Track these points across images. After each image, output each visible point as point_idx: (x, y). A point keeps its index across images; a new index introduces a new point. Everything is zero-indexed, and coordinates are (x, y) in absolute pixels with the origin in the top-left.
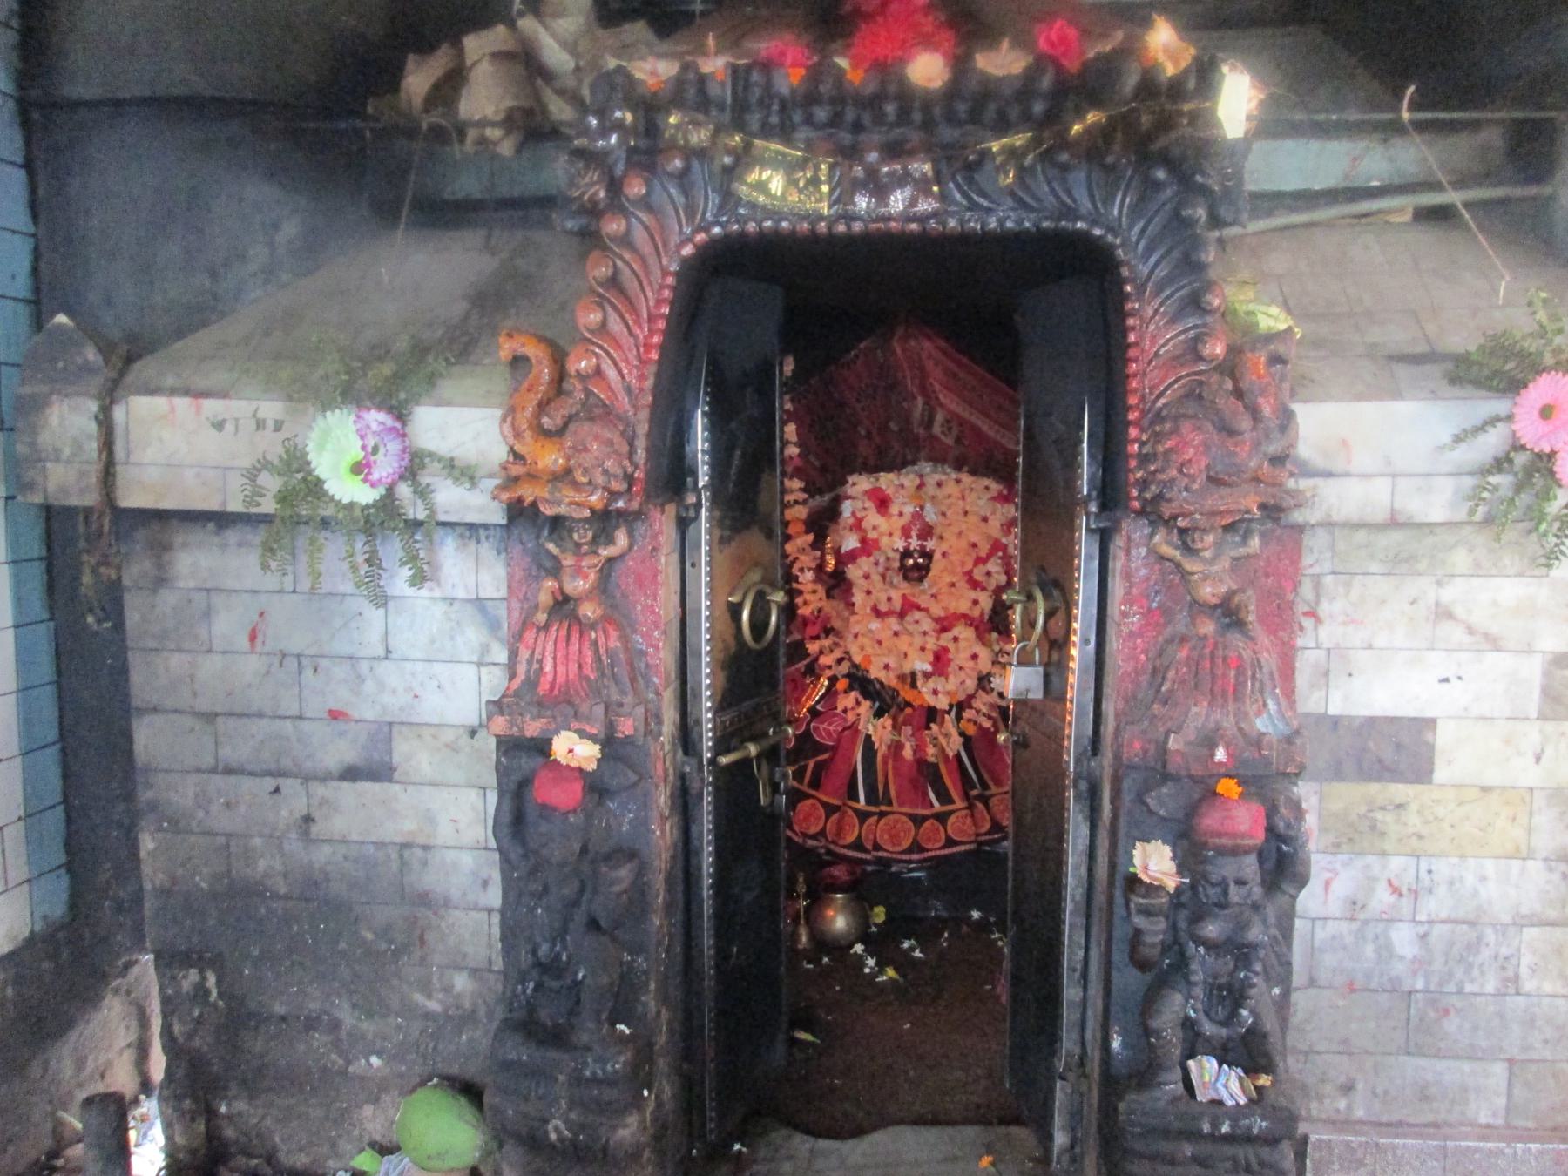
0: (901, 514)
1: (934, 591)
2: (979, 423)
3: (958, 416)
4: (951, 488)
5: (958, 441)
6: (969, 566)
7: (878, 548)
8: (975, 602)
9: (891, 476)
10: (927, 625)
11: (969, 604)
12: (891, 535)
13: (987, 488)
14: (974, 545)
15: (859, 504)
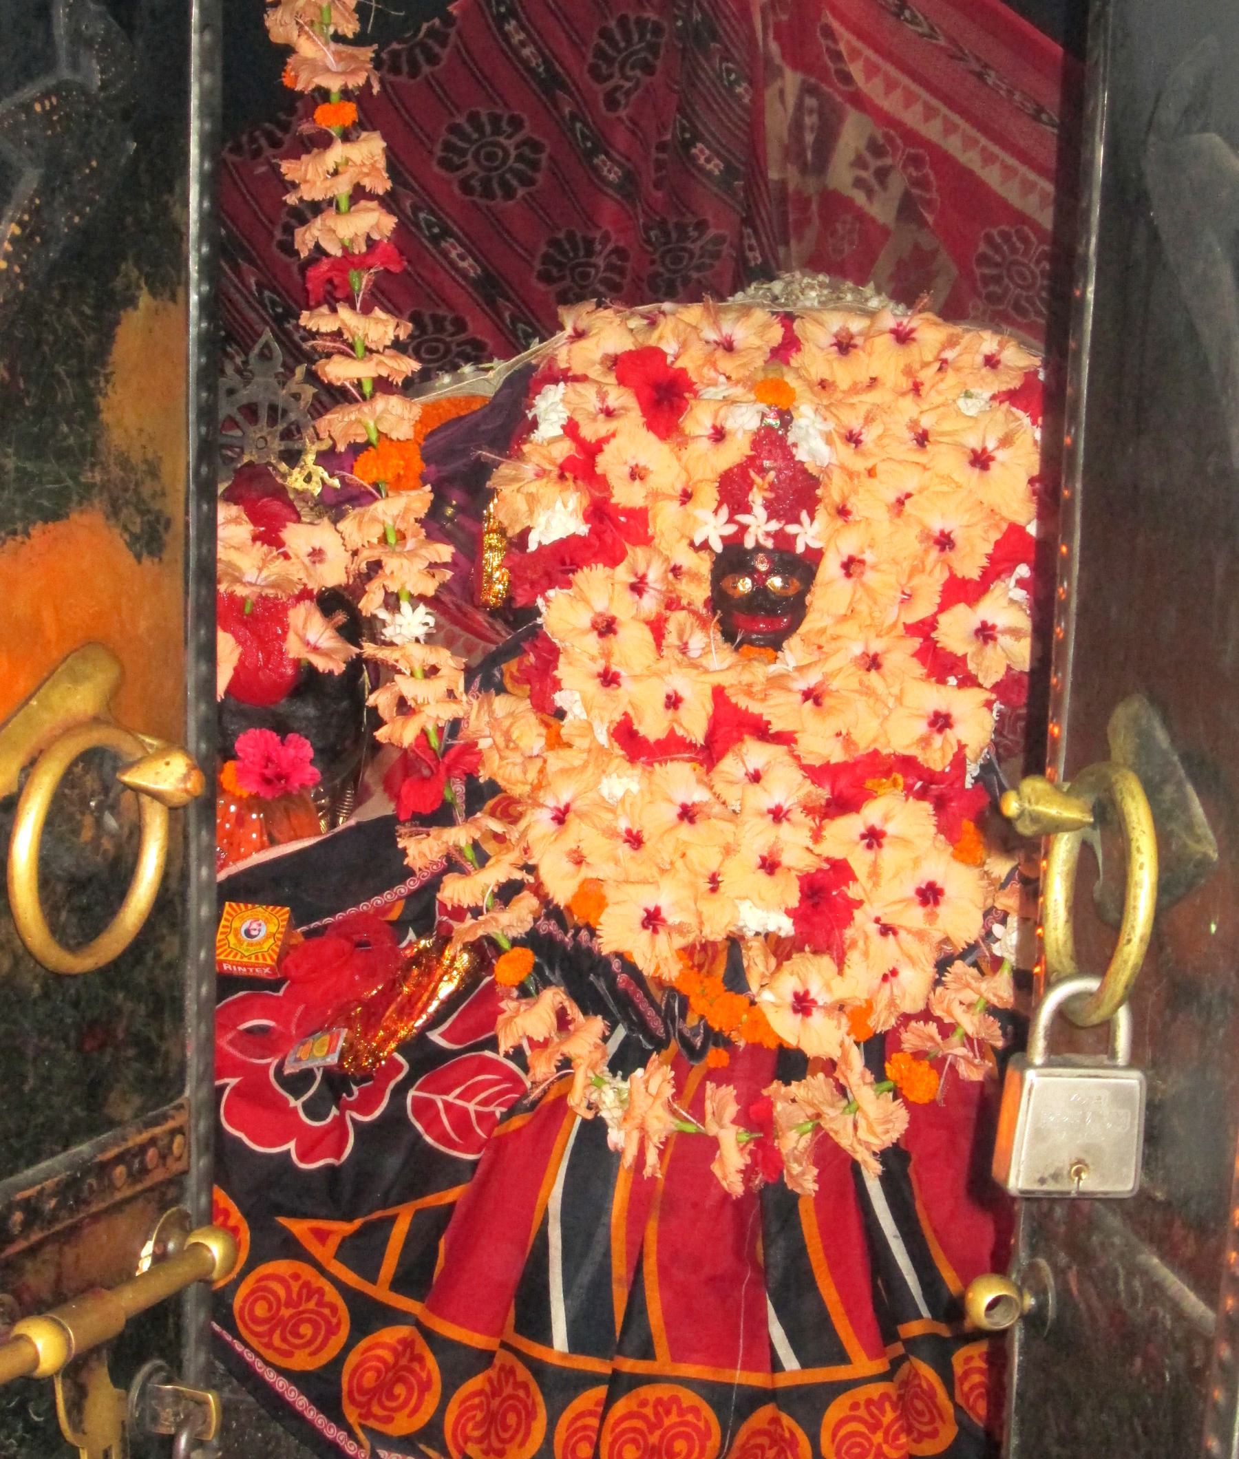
0: (719, 435)
1: (811, 680)
2: (970, 159)
3: (911, 137)
4: (882, 359)
5: (908, 209)
6: (923, 609)
7: (646, 540)
8: (941, 722)
9: (693, 313)
10: (786, 786)
11: (921, 728)
12: (686, 497)
13: (991, 362)
14: (945, 542)
15: (589, 397)
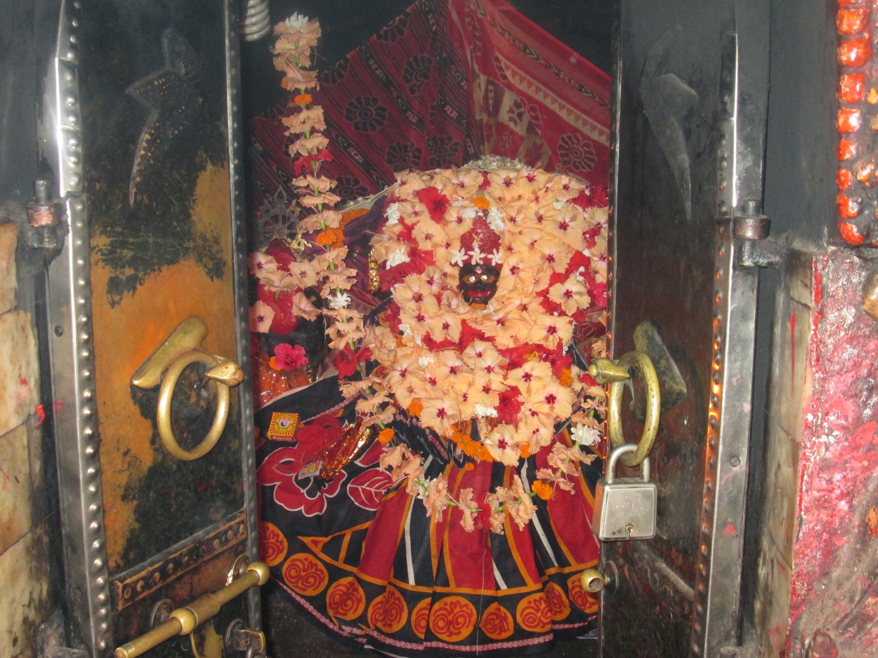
0: (460, 220)
1: (500, 315)
2: (555, 108)
3: (530, 99)
5: (530, 129)
7: (433, 263)
8: (552, 330)
9: (448, 173)
10: (492, 358)
11: (544, 333)
12: (448, 245)
13: (566, 187)
14: (550, 259)
15: (408, 208)
